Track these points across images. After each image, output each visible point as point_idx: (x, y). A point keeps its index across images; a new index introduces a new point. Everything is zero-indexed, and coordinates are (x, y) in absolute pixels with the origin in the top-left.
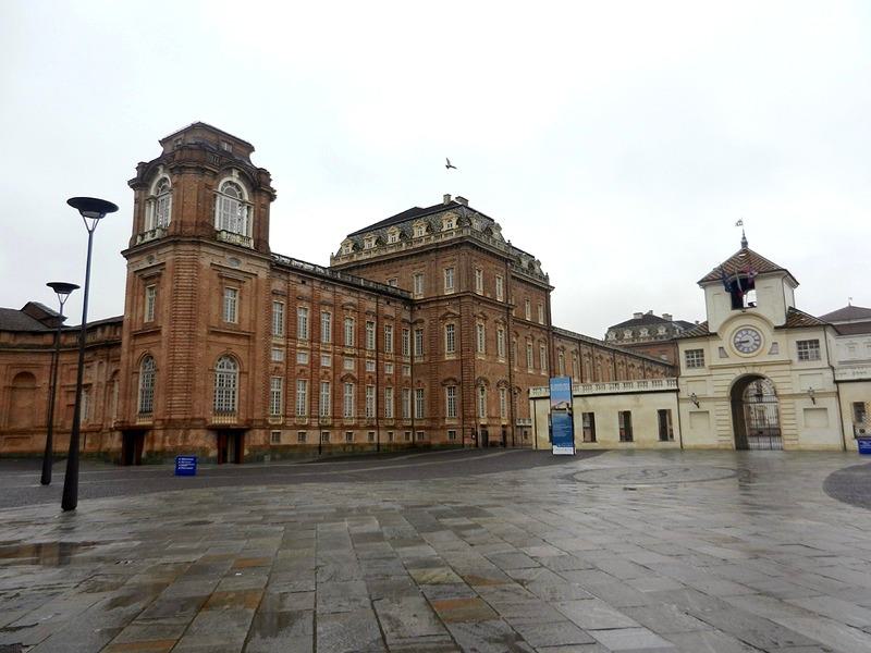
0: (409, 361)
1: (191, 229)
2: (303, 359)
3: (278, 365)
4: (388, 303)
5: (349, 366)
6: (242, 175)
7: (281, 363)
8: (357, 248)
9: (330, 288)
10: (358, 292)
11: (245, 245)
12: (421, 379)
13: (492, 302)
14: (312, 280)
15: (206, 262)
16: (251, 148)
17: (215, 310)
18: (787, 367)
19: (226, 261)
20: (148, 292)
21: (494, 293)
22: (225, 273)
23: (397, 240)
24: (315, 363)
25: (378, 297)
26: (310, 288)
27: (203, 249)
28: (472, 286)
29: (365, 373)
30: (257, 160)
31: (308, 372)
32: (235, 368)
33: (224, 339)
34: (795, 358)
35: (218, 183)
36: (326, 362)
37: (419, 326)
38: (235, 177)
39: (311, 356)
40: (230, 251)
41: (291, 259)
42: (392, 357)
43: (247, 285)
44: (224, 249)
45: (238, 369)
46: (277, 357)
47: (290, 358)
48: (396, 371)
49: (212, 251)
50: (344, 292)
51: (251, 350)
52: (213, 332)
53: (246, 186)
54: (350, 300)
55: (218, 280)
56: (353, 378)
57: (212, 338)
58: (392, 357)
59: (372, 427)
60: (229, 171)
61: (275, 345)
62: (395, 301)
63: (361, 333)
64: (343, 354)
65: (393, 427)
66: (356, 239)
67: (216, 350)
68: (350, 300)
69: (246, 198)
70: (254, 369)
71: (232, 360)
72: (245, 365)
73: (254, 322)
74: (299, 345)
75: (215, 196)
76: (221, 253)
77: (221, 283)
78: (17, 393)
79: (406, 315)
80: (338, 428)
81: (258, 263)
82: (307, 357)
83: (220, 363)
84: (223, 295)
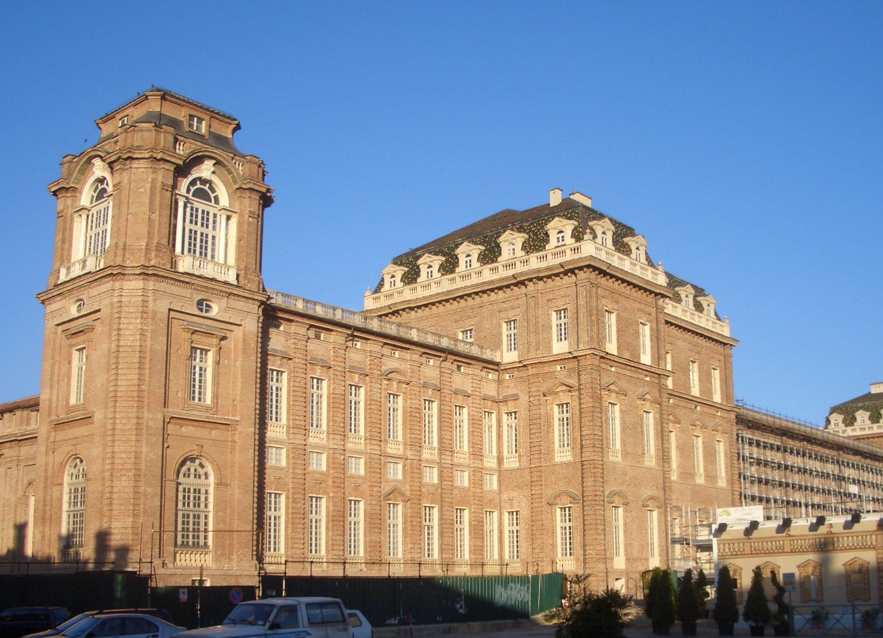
2: (320, 463)
4: (459, 367)
5: (396, 472)
11: (222, 278)
12: (514, 494)
13: (634, 365)
20: (76, 355)
21: (636, 351)
28: (601, 339)
33: (187, 430)
37: (511, 406)
48: (441, 476)
69: (224, 201)
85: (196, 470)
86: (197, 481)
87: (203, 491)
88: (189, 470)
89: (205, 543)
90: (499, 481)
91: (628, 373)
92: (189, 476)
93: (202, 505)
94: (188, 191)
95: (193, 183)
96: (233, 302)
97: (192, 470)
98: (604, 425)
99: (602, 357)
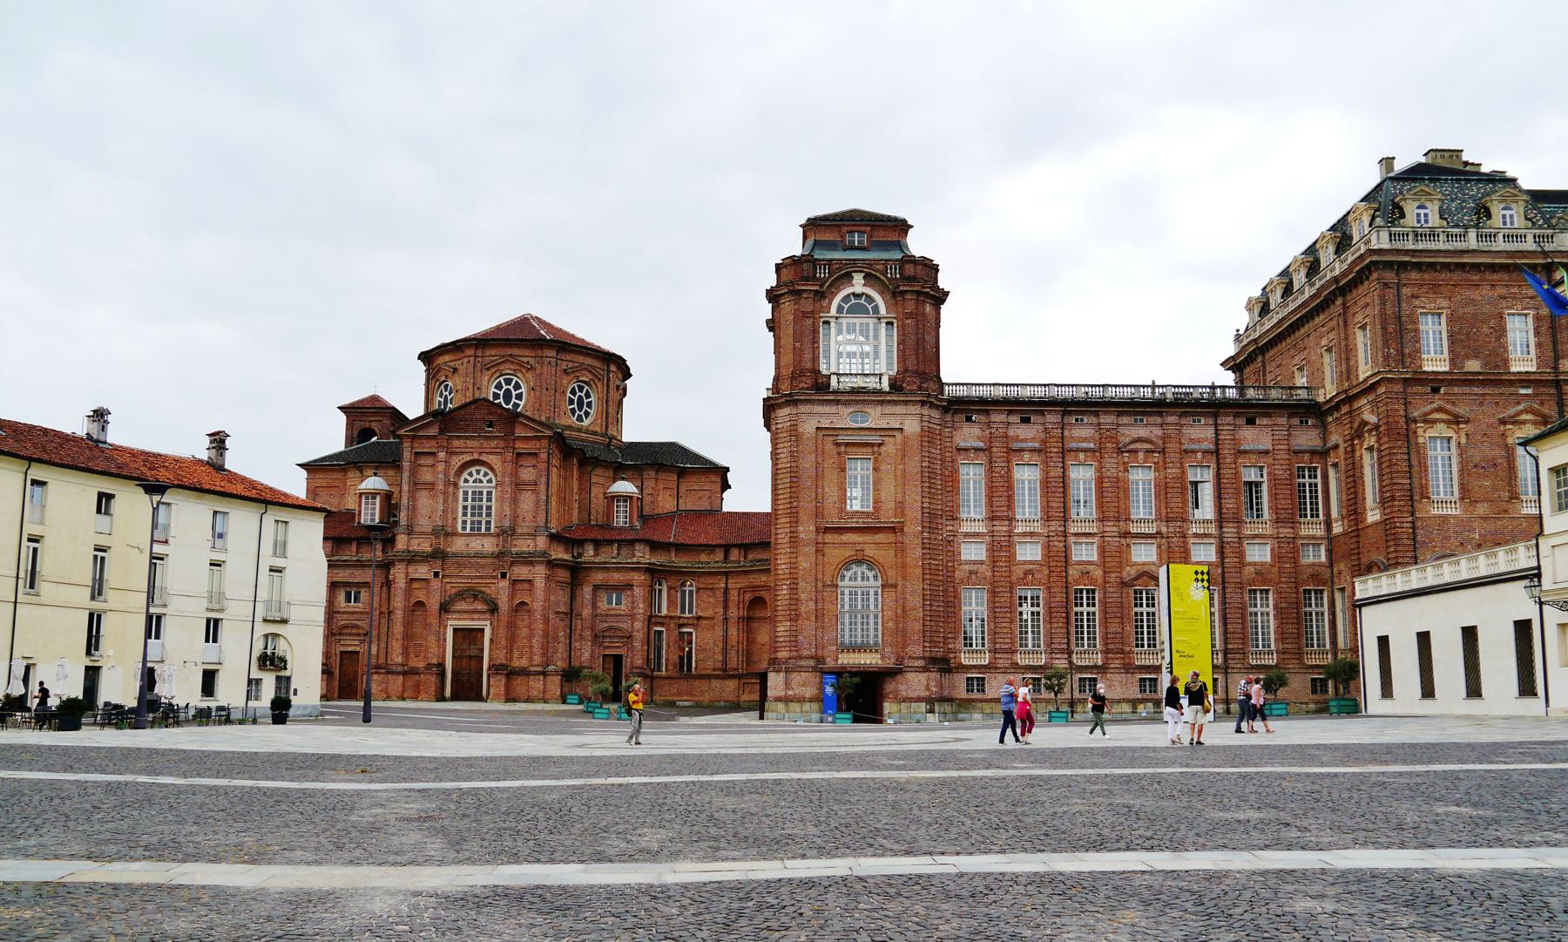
0: (1319, 531)
1: (785, 388)
2: (1029, 552)
3: (974, 568)
6: (869, 278)
7: (981, 563)
8: (1265, 309)
9: (1094, 420)
10: (1160, 414)
14: (1042, 413)
15: (808, 427)
16: (902, 226)
17: (831, 492)
19: (844, 417)
21: (1498, 356)
22: (842, 439)
23: (1304, 280)
24: (1057, 558)
25: (1216, 416)
26: (1041, 428)
27: (803, 408)
33: (845, 538)
35: (830, 303)
36: (1085, 553)
38: (858, 284)
39: (1047, 548)
40: (847, 403)
43: (890, 448)
44: (837, 402)
45: (879, 583)
46: (973, 552)
47: (1001, 549)
50: (1125, 420)
51: (901, 549)
52: (827, 530)
53: (881, 293)
54: (1142, 432)
55: (834, 450)
57: (829, 538)
60: (847, 278)
67: (835, 555)
68: (1142, 432)
69: (883, 311)
70: (904, 578)
72: (891, 573)
73: (901, 506)
74: (1019, 530)
75: (828, 323)
77: (839, 454)
78: (755, 625)
79: (1307, 438)
80: (1117, 671)
81: (899, 409)
82: (1039, 546)
83: (848, 574)
84: (843, 470)
85: (863, 573)
86: (865, 583)
87: (872, 592)
90: (1329, 552)
91: (1475, 390)
92: (855, 579)
94: (840, 309)
95: (846, 299)
96: (889, 409)
97: (859, 574)
98: (1416, 468)
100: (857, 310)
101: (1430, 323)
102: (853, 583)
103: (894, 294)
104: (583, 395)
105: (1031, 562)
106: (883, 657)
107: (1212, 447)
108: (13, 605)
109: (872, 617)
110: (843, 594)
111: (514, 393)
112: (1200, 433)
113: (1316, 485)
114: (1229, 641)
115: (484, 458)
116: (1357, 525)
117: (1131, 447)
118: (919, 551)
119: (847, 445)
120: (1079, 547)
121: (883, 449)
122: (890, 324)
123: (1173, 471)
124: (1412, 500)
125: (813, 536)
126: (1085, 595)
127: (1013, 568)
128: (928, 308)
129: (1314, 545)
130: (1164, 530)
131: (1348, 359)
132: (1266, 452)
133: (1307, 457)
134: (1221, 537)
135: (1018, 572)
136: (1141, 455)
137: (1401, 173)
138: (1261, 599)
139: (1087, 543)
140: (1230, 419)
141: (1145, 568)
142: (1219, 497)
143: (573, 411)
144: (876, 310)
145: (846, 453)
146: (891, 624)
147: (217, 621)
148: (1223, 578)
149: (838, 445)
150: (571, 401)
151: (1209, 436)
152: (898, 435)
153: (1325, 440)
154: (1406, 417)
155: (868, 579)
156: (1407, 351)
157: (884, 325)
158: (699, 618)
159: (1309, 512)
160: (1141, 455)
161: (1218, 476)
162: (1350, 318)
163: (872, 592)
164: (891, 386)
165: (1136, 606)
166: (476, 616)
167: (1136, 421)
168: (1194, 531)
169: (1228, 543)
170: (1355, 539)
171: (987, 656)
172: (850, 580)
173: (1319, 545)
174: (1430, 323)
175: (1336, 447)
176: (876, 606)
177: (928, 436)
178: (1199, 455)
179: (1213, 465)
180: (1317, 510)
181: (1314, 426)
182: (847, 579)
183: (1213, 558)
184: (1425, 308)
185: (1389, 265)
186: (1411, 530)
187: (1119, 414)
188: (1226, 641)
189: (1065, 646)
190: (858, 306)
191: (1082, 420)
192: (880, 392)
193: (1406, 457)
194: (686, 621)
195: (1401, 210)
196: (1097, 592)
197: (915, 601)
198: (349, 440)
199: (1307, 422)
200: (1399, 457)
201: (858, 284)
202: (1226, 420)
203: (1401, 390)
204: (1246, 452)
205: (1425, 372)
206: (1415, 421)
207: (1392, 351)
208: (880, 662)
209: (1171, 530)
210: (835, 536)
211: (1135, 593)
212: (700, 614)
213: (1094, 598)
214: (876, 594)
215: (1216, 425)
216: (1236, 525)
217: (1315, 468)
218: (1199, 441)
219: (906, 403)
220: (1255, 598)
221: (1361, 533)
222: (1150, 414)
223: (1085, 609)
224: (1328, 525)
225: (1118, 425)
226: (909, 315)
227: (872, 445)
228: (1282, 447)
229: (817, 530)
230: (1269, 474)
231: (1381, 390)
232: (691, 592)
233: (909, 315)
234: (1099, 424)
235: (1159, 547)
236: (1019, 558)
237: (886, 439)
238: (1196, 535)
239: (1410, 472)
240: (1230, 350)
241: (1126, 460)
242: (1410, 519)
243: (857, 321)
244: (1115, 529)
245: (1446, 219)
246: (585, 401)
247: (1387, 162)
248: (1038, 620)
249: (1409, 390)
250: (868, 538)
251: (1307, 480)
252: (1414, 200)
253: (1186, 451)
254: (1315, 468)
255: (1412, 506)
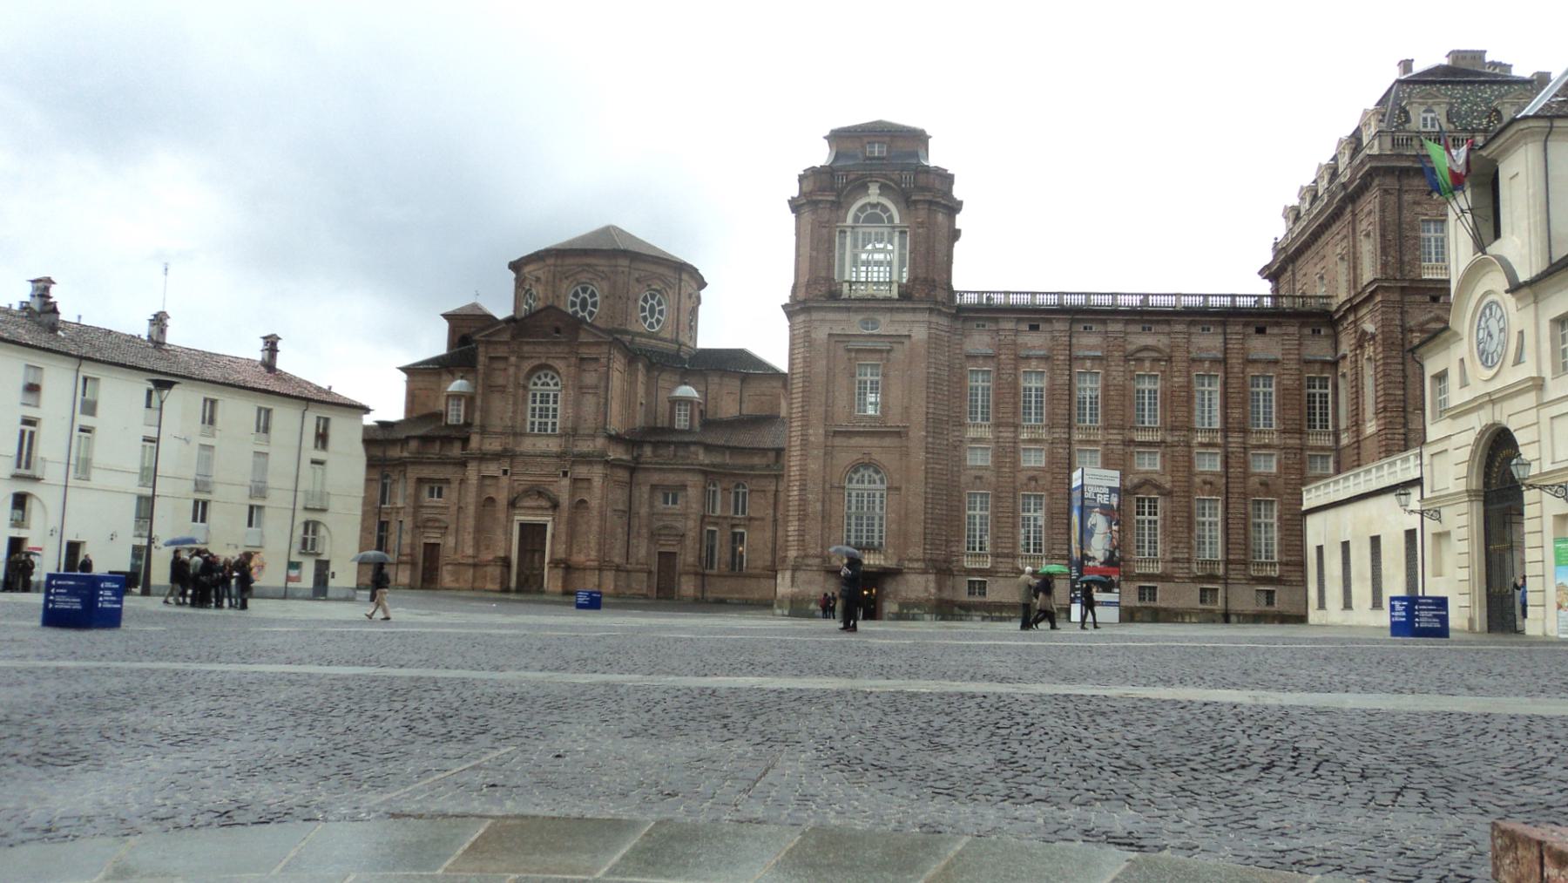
3: (980, 473)
6: (884, 189)
7: (986, 468)
9: (1100, 328)
10: (1168, 322)
14: (1049, 321)
17: (841, 400)
18: (1530, 399)
19: (853, 325)
25: (1224, 324)
26: (1048, 336)
27: (815, 316)
29: (1246, 475)
30: (936, 157)
31: (1046, 480)
32: (882, 481)
34: (1547, 372)
38: (874, 195)
40: (857, 310)
41: (1007, 293)
42: (1275, 439)
43: (899, 354)
44: (848, 309)
45: (884, 487)
47: (1007, 454)
49: (831, 316)
50: (1132, 328)
51: (905, 453)
52: (836, 433)
53: (896, 203)
54: (1149, 340)
56: (1158, 487)
57: (838, 441)
58: (1275, 439)
59: (1212, 578)
60: (863, 188)
61: (974, 440)
62: (1278, 324)
63: (1180, 402)
64: (1132, 442)
65: (1278, 581)
66: (1294, 214)
67: (844, 459)
68: (1149, 340)
69: (897, 221)
71: (877, 472)
74: (1025, 436)
75: (843, 232)
76: (843, 316)
79: (1319, 349)
81: (908, 317)
83: (856, 477)
85: (870, 476)
86: (872, 486)
87: (878, 495)
88: (863, 476)
89: (881, 544)
92: (863, 482)
93: (877, 509)
94: (856, 219)
95: (863, 208)
96: (899, 317)
99: (1403, 288)
100: (870, 219)
101: (1432, 230)
102: (860, 486)
103: (906, 200)
104: (655, 303)
105: (1035, 469)
106: (886, 559)
107: (1220, 356)
108: (63, 488)
109: (877, 519)
110: (850, 495)
111: (589, 301)
112: (1209, 342)
113: (1326, 395)
114: (1230, 551)
115: (550, 362)
116: (1358, 436)
117: (1139, 355)
118: (922, 456)
119: (858, 351)
120: (1082, 454)
121: (893, 355)
122: (902, 233)
123: (1179, 380)
124: (1404, 410)
125: (822, 439)
126: (1147, 504)
127: (1018, 475)
128: (940, 217)
129: (1322, 456)
130: (1169, 439)
131: (1355, 268)
132: (1276, 362)
133: (1317, 367)
134: (1225, 446)
135: (1022, 477)
136: (1147, 364)
137: (1419, 75)
138: (1265, 510)
139: (1150, 453)
140: (1238, 328)
141: (1149, 476)
142: (1225, 406)
143: (645, 319)
144: (891, 219)
145: (856, 359)
146: (894, 526)
147: (205, 504)
148: (1227, 488)
149: (849, 351)
150: (643, 309)
151: (1218, 345)
152: (906, 341)
153: (1336, 349)
154: (1401, 326)
155: (875, 482)
156: (1406, 259)
157: (897, 234)
158: (751, 519)
159: (1318, 423)
160: (1147, 364)
161: (1225, 385)
162: (1358, 226)
163: (878, 495)
164: (899, 295)
165: (1138, 514)
166: (539, 512)
167: (1144, 329)
168: (1199, 439)
169: (1233, 453)
170: (1356, 451)
171: (989, 560)
172: (858, 482)
173: (1328, 456)
174: (1432, 230)
175: (1344, 357)
176: (881, 508)
177: (934, 341)
178: (1207, 364)
179: (1221, 374)
180: (1327, 421)
181: (1326, 336)
182: (854, 481)
183: (1218, 468)
184: (1426, 215)
185: (1389, 171)
186: (1403, 442)
187: (1127, 322)
188: (1227, 551)
189: (1065, 552)
190: (874, 216)
191: (1091, 328)
192: (889, 299)
193: (1400, 367)
194: (737, 522)
195: (1406, 113)
196: (1159, 501)
197: (917, 503)
198: (452, 343)
199: (1319, 331)
200: (1393, 367)
201: (874, 195)
202: (1235, 329)
203: (1398, 299)
204: (1254, 361)
205: (1425, 280)
206: (1412, 331)
207: (1390, 258)
208: (883, 563)
209: (1176, 439)
210: (844, 439)
211: (1138, 499)
212: (752, 515)
213: (1155, 507)
214: (882, 496)
215: (1225, 333)
216: (1241, 435)
217: (1326, 379)
218: (1207, 350)
219: (914, 310)
220: (1259, 510)
221: (1362, 444)
222: (1158, 322)
223: (1147, 518)
224: (1337, 435)
225: (1126, 333)
226: (921, 225)
227: (881, 351)
228: (1291, 357)
229: (826, 435)
230: (1278, 383)
231: (1378, 298)
232: (744, 494)
233: (921, 225)
234: (1106, 332)
235: (1163, 456)
236: (1024, 464)
237: (895, 345)
238: (1202, 445)
239: (1404, 383)
240: (1267, 257)
241: (1133, 368)
242: (1402, 431)
243: (873, 231)
244: (1120, 437)
245: (1453, 123)
246: (657, 309)
247: (1406, 65)
248: (1155, 529)
249: (1407, 299)
250: (875, 441)
251: (1317, 391)
252: (1421, 104)
253: (1194, 360)
254: (1327, 378)
255: (1404, 417)
